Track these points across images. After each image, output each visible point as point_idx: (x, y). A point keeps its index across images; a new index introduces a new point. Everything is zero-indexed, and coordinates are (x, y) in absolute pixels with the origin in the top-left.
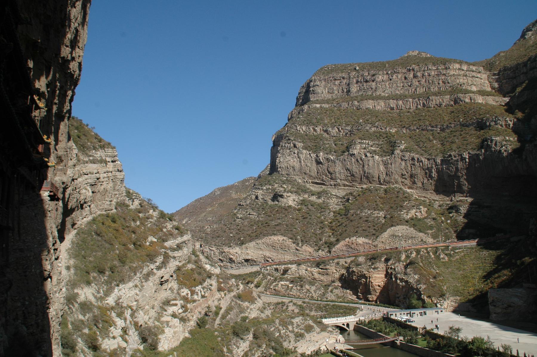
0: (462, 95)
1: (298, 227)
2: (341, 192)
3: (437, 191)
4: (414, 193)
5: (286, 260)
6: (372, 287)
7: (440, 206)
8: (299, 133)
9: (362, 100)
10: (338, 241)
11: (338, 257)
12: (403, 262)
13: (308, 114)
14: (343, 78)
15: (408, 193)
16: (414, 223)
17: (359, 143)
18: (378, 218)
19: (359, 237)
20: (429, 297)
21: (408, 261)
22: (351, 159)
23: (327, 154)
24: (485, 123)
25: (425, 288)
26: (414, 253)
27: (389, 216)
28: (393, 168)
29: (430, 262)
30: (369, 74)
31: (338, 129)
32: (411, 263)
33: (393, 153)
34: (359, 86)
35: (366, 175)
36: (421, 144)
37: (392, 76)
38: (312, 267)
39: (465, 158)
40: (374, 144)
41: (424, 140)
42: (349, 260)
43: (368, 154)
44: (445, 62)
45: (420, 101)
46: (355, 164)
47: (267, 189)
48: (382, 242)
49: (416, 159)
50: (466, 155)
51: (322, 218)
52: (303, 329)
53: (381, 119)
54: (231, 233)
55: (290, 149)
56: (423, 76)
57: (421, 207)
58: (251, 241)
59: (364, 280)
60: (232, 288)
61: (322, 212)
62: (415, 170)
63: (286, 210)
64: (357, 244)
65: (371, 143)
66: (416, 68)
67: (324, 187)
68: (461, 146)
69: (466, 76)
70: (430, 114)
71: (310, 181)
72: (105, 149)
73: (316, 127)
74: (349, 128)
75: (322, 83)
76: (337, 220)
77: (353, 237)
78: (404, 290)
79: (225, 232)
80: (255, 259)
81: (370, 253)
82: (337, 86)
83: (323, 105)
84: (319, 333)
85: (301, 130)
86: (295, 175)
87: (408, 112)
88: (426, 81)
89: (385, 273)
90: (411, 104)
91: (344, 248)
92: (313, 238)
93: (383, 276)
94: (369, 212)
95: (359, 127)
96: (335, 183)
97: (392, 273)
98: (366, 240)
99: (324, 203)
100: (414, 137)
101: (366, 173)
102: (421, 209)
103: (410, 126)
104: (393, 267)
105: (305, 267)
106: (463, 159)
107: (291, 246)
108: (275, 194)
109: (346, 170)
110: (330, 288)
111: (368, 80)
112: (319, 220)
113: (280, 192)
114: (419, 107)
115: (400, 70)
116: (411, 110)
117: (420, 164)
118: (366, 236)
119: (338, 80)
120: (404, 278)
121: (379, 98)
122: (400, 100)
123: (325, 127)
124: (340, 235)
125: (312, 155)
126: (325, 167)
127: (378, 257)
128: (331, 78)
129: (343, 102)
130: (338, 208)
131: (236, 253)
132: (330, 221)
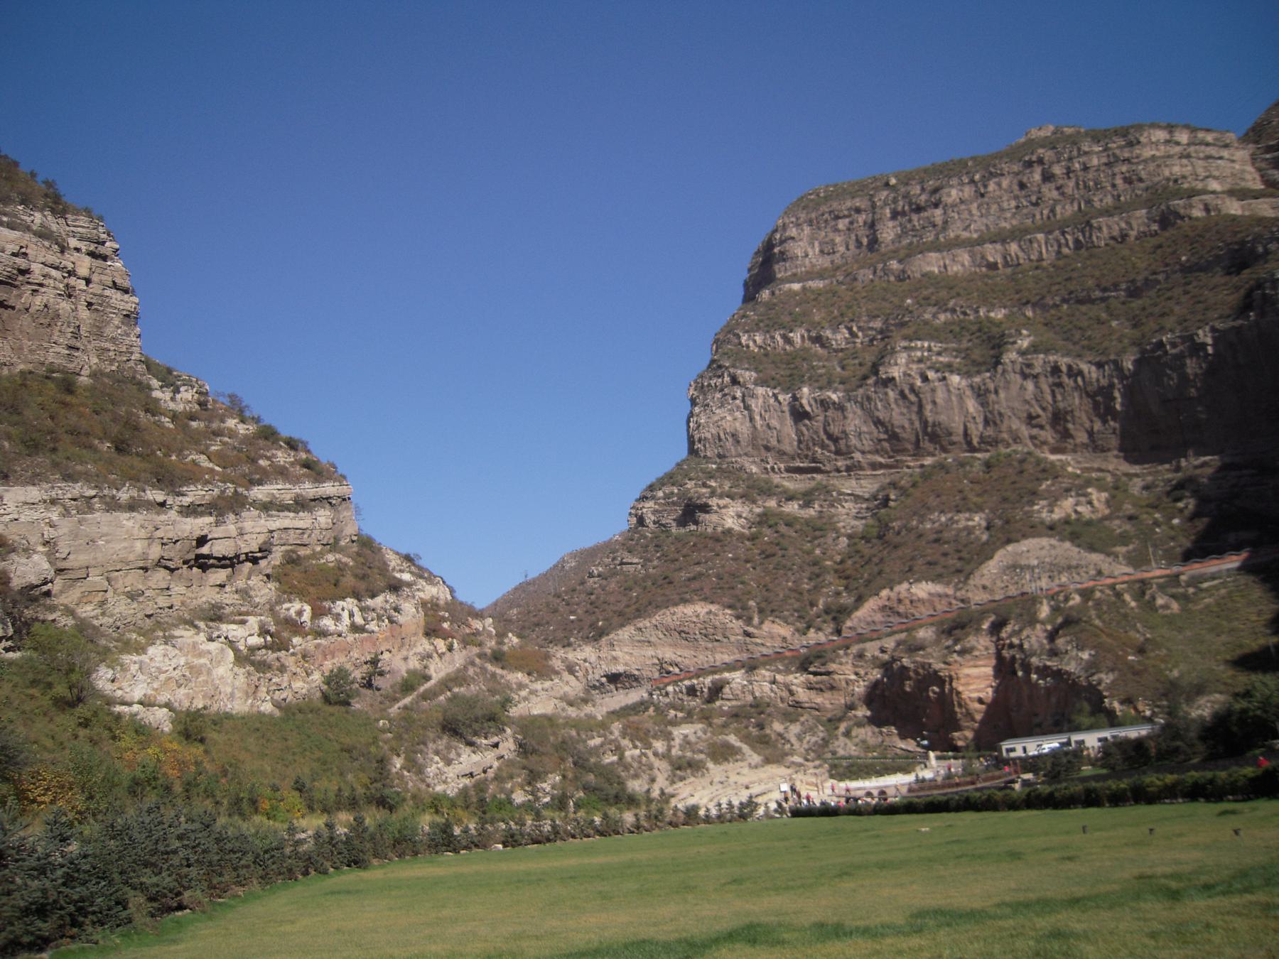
0: (1181, 202)
1: (752, 580)
2: (867, 486)
3: (1132, 452)
4: (1071, 463)
5: (718, 664)
6: (960, 706)
7: (1146, 488)
8: (745, 352)
9: (908, 256)
10: (860, 600)
11: (861, 638)
12: (1043, 623)
13: (770, 306)
14: (858, 211)
15: (1052, 463)
16: (1073, 530)
17: (905, 348)
18: (970, 530)
19: (918, 581)
20: (1128, 701)
21: (1060, 620)
22: (886, 394)
23: (821, 388)
24: (1253, 250)
25: (1113, 682)
26: (1073, 599)
27: (998, 522)
28: (1003, 401)
29: (1125, 616)
30: (923, 189)
31: (850, 330)
32: (1068, 622)
33: (998, 363)
34: (901, 225)
35: (929, 429)
36: (1077, 335)
37: (985, 186)
38: (787, 672)
39: (1204, 345)
40: (946, 350)
41: (1085, 324)
42: (890, 643)
43: (931, 375)
44: (1128, 134)
45: (1068, 237)
46: (898, 405)
47: (667, 496)
48: (984, 587)
49: (1064, 369)
50: (1204, 335)
51: (818, 552)
52: (701, 752)
53: (962, 292)
54: (572, 613)
55: (722, 390)
56: (1068, 174)
57: (1090, 490)
58: (622, 626)
59: (936, 689)
60: (480, 638)
61: (816, 538)
62: (1064, 399)
63: (718, 540)
64: (911, 602)
65: (936, 347)
66: (1048, 155)
67: (818, 477)
68: (1188, 317)
69: (1188, 156)
70: (1094, 261)
71: (782, 466)
72: (67, 216)
73: (791, 332)
74: (878, 324)
75: (802, 230)
76: (858, 552)
77: (900, 583)
78: (1053, 700)
79: (556, 611)
80: (636, 673)
81: (949, 616)
82: (842, 233)
83: (810, 284)
84: (756, 767)
85: (751, 344)
86: (740, 456)
87: (1037, 268)
88: (1077, 184)
89: (993, 662)
90: (1043, 246)
91: (878, 617)
92: (793, 601)
93: (989, 671)
94: (943, 519)
95: (904, 316)
96: (848, 462)
97: (1013, 658)
98: (938, 588)
99: (820, 518)
100: (1055, 323)
101: (930, 424)
102: (1090, 494)
103: (1043, 298)
104: (1016, 641)
105: (767, 674)
106: (1196, 348)
107: (730, 625)
108: (687, 506)
109: (875, 424)
110: (843, 727)
111: (923, 204)
112: (808, 559)
113: (698, 498)
114: (1065, 251)
115: (1006, 167)
116: (1045, 264)
117: (1076, 381)
118: (937, 578)
119: (845, 217)
120: (1049, 663)
121: (957, 243)
122: (1012, 240)
123: (815, 328)
124: (866, 586)
125: (781, 397)
126: (818, 424)
127: (970, 621)
128: (826, 216)
129: (862, 267)
130: (859, 525)
131: (585, 661)
132: (838, 558)
